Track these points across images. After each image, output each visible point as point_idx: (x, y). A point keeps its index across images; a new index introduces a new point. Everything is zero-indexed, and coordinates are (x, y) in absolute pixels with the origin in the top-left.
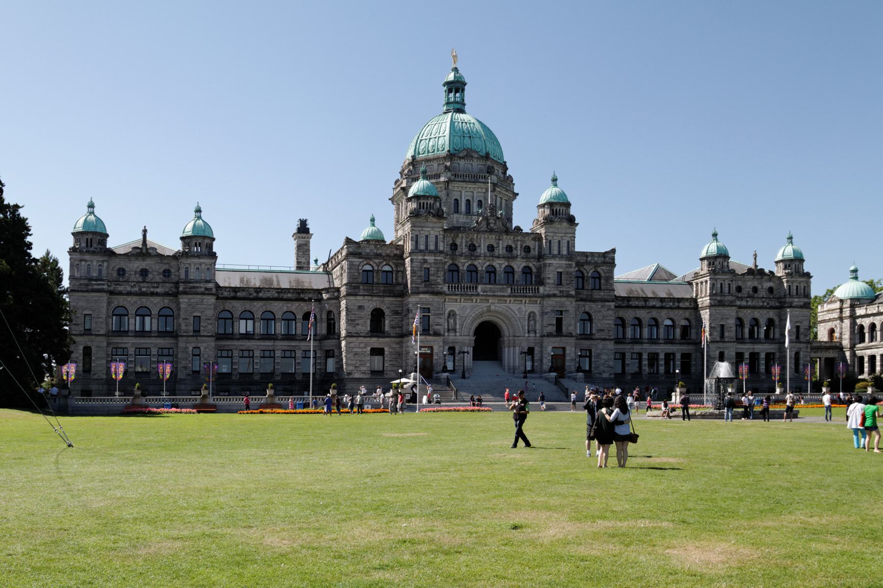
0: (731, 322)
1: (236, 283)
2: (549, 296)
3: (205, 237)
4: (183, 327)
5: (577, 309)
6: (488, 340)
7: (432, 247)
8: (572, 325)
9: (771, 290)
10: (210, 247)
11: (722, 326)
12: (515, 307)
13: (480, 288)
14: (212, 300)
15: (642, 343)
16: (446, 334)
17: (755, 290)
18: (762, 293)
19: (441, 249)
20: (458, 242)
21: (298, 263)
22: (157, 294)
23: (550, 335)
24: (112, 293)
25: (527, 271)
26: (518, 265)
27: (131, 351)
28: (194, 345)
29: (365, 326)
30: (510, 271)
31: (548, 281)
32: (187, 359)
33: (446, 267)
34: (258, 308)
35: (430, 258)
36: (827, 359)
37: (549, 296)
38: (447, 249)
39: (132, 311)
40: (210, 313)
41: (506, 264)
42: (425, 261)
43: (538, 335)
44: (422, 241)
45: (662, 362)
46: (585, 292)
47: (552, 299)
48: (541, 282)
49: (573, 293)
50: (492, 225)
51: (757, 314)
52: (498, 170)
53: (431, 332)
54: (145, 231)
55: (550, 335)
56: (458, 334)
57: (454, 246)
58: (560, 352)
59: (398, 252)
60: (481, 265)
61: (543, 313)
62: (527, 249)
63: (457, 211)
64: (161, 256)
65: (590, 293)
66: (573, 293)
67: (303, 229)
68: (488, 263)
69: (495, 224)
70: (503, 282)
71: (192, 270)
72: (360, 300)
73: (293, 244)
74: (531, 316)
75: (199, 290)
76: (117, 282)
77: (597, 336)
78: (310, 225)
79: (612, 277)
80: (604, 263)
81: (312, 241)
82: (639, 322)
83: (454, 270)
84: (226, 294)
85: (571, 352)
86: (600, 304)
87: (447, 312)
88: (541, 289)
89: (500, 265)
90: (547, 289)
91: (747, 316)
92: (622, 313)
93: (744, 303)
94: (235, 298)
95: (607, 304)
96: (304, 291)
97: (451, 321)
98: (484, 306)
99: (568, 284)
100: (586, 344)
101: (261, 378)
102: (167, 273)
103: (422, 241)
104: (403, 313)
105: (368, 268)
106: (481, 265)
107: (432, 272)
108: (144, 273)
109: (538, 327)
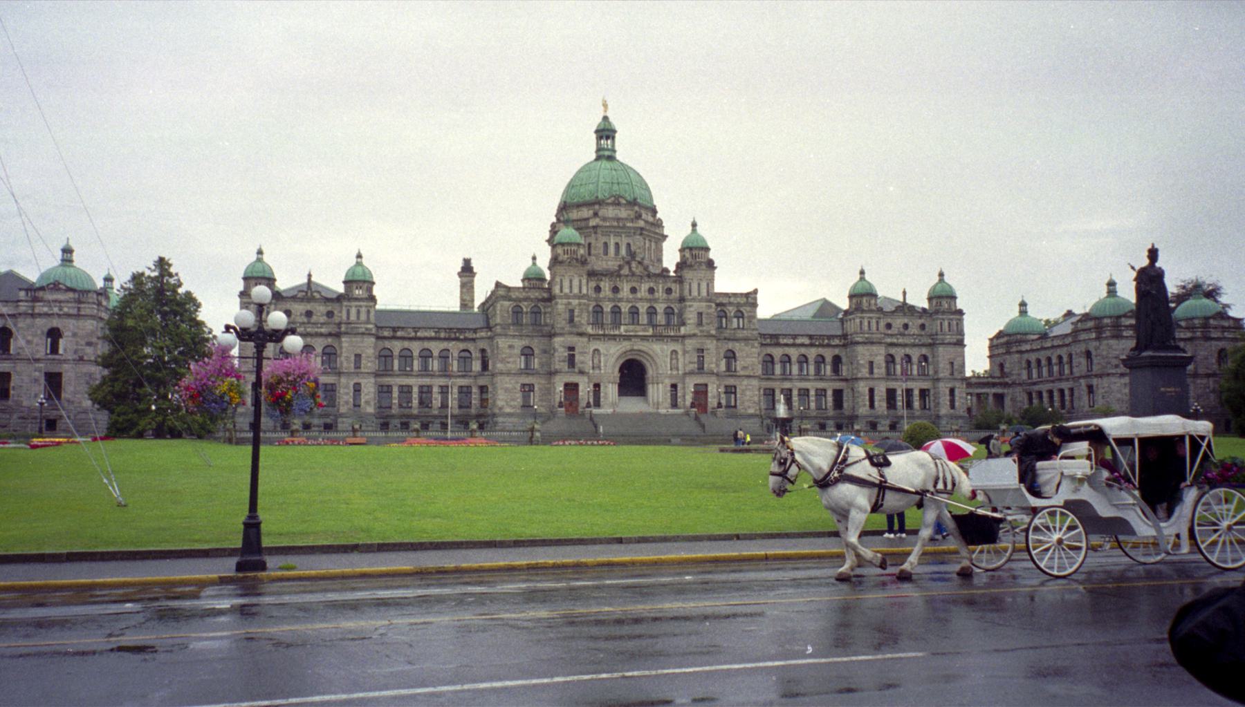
0: (880, 360)
3: (364, 282)
4: (345, 364)
5: (717, 348)
7: (576, 290)
8: (711, 363)
9: (923, 327)
10: (370, 290)
11: (871, 363)
13: (622, 328)
14: (373, 340)
15: (791, 380)
17: (906, 326)
18: (914, 330)
19: (584, 291)
20: (602, 284)
21: (462, 300)
22: (321, 335)
23: (691, 373)
25: (669, 312)
26: (660, 308)
28: (356, 380)
30: (652, 312)
32: (347, 394)
33: (591, 309)
36: (995, 395)
40: (370, 351)
42: (569, 304)
44: (566, 284)
45: (812, 398)
48: (684, 324)
49: (713, 332)
51: (908, 351)
52: (647, 216)
54: (310, 276)
55: (691, 373)
57: (598, 289)
58: (702, 389)
59: (545, 295)
61: (685, 352)
62: (669, 291)
63: (606, 253)
64: (327, 300)
67: (467, 270)
70: (645, 322)
71: (353, 311)
72: (511, 341)
73: (457, 281)
75: (361, 330)
77: (742, 373)
78: (474, 264)
79: (754, 317)
80: (747, 304)
81: (476, 279)
82: (787, 359)
83: (598, 310)
84: (386, 334)
85: (713, 390)
88: (682, 329)
89: (643, 308)
90: (688, 328)
91: (899, 353)
92: (770, 350)
93: (895, 341)
94: (394, 338)
96: (460, 330)
97: (596, 361)
98: (626, 345)
102: (330, 314)
103: (566, 284)
104: (548, 352)
106: (625, 308)
108: (309, 314)
109: (680, 366)
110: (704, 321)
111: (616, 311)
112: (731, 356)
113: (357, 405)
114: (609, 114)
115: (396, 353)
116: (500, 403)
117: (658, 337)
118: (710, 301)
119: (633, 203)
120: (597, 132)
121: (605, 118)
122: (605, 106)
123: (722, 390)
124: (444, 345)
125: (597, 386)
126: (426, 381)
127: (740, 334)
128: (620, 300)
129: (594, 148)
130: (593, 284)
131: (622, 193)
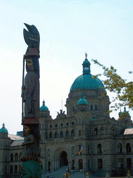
2: (76, 140)
6: (63, 158)
12: (67, 145)
16: (47, 157)
25: (73, 132)
26: (70, 130)
31: (76, 134)
33: (49, 134)
37: (76, 140)
38: (49, 127)
41: (66, 130)
43: (75, 155)
46: (98, 136)
47: (77, 141)
48: (74, 136)
50: (61, 117)
53: (41, 157)
56: (50, 157)
57: (51, 126)
60: (59, 131)
62: (73, 123)
65: (100, 136)
66: (85, 138)
68: (61, 131)
69: (62, 116)
74: (73, 148)
77: (104, 153)
83: (51, 134)
84: (12, 148)
85: (84, 162)
86: (104, 140)
87: (47, 150)
89: (64, 130)
94: (14, 149)
95: (106, 140)
99: (83, 135)
100: (100, 157)
101: (19, 174)
106: (59, 131)
107: (41, 136)
110: (81, 134)
111: (56, 134)
114: (87, 58)
115: (14, 154)
118: (82, 125)
119: (84, 89)
121: (86, 60)
122: (86, 55)
123: (97, 160)
125: (49, 163)
127: (102, 137)
129: (82, 71)
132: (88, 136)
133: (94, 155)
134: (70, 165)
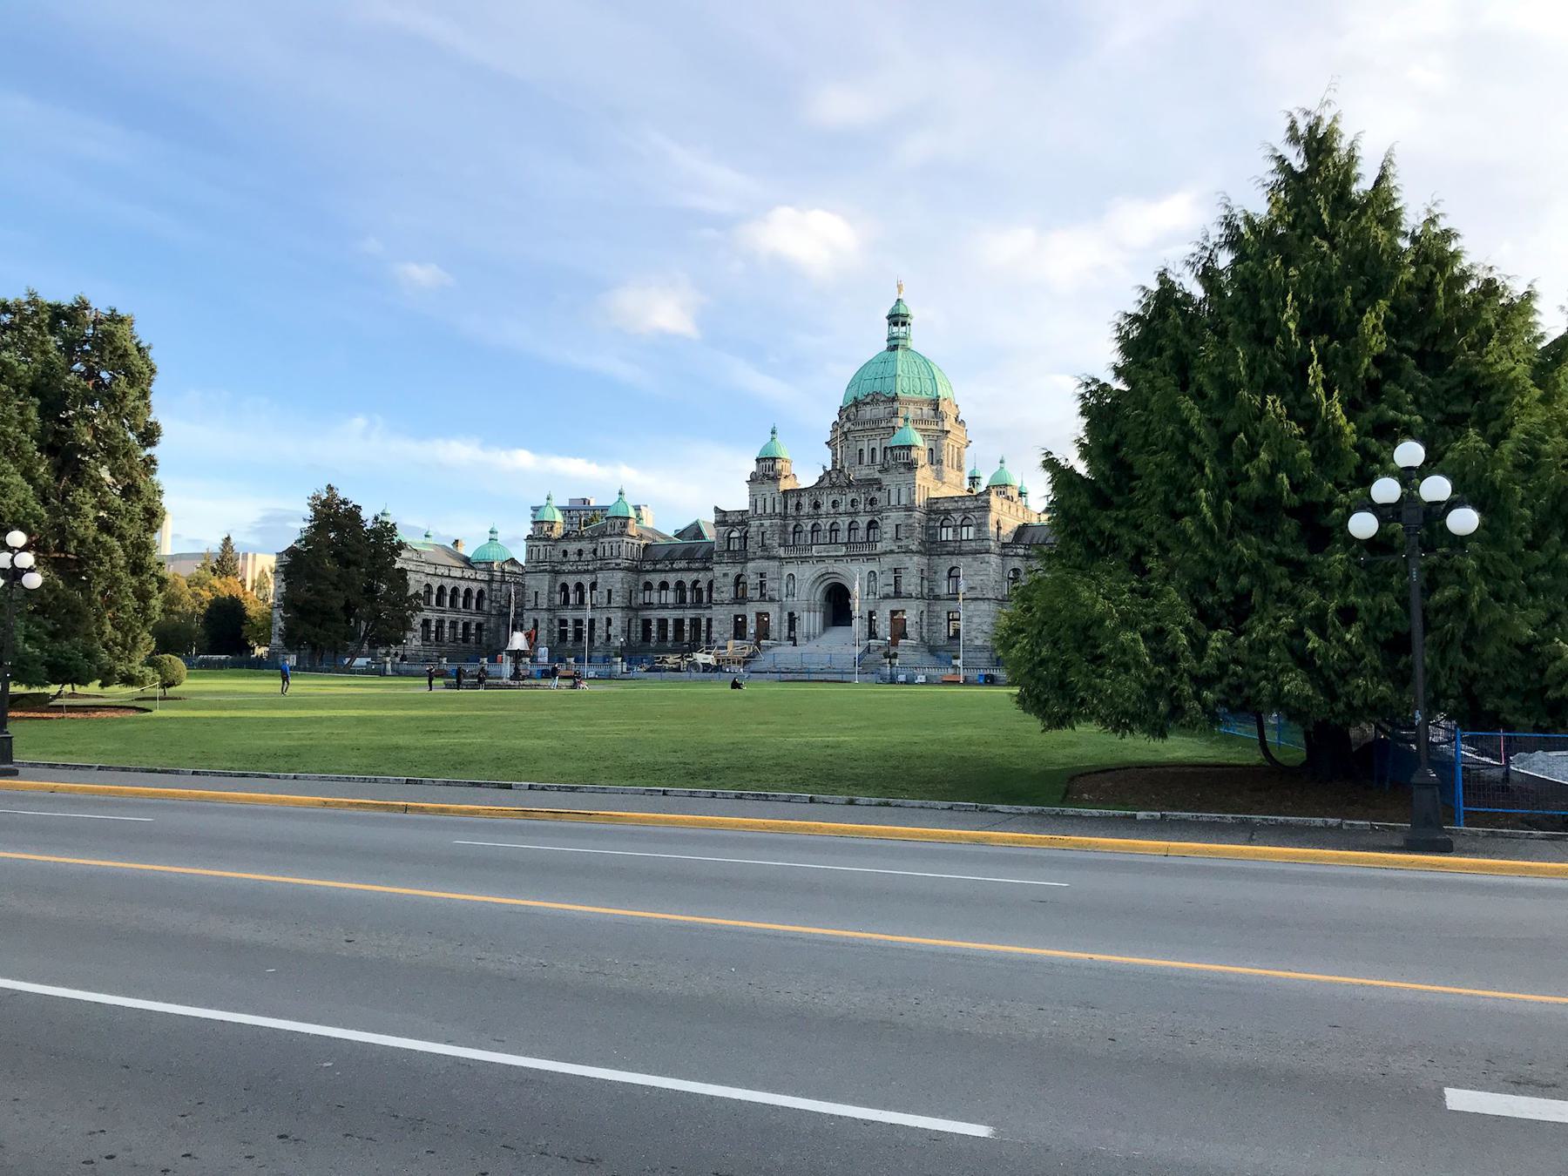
1: (661, 556)
2: (885, 553)
8: (911, 584)
23: (887, 597)
24: (558, 573)
25: (872, 525)
26: (863, 521)
27: (570, 622)
29: (728, 593)
33: (791, 529)
34: (672, 579)
35: (767, 523)
37: (885, 553)
38: (791, 510)
39: (572, 588)
49: (914, 548)
55: (887, 597)
62: (872, 501)
76: (562, 563)
85: (911, 616)
86: (970, 559)
89: (844, 522)
94: (654, 571)
98: (821, 568)
102: (595, 551)
105: (733, 535)
106: (825, 524)
108: (580, 552)
111: (815, 529)
112: (952, 574)
113: (609, 637)
116: (714, 636)
117: (853, 557)
119: (894, 399)
120: (889, 317)
122: (900, 287)
124: (694, 576)
125: (791, 614)
126: (678, 614)
127: (966, 547)
128: (819, 516)
130: (792, 502)
131: (885, 390)
132: (922, 543)
133: (937, 598)
134: (858, 627)
